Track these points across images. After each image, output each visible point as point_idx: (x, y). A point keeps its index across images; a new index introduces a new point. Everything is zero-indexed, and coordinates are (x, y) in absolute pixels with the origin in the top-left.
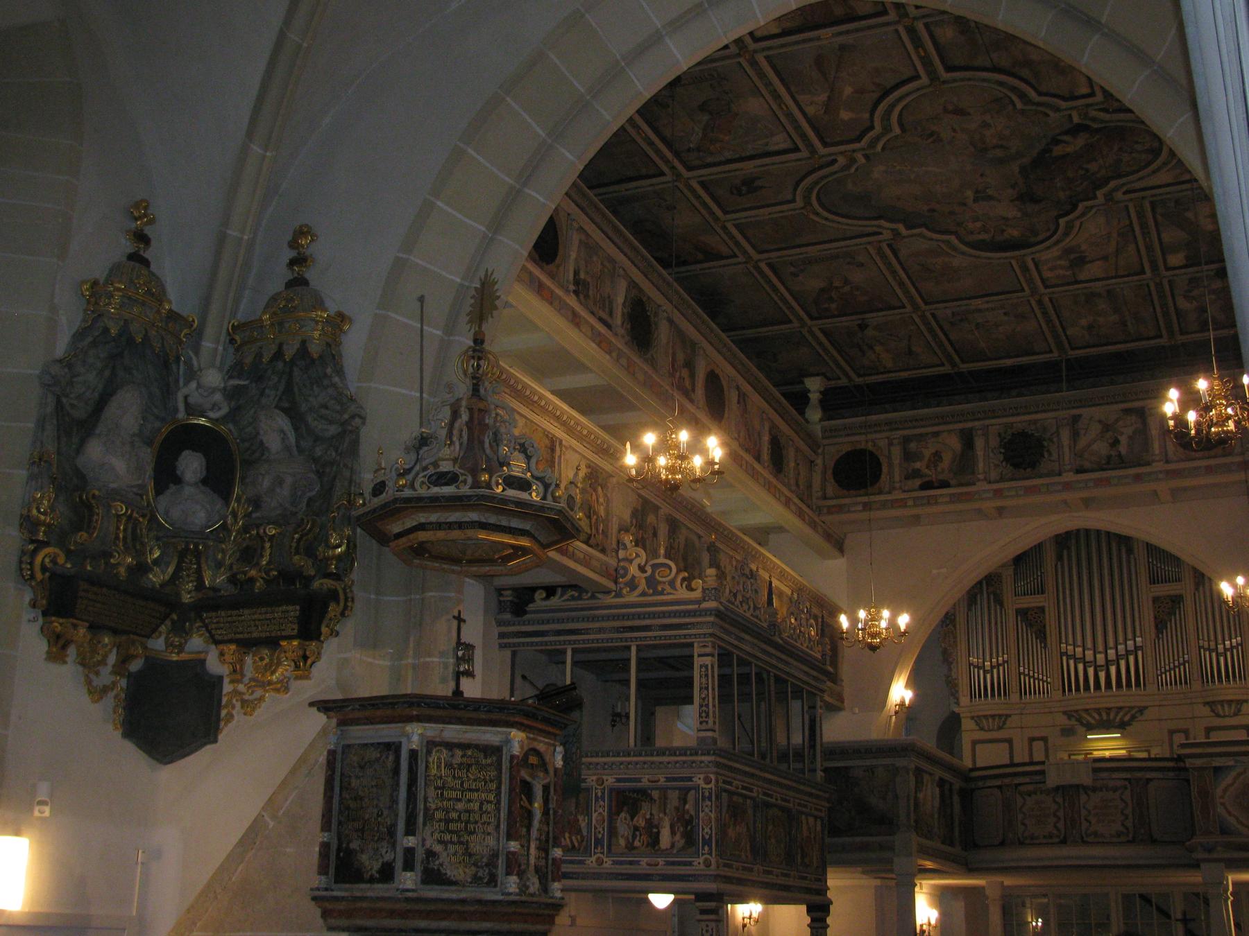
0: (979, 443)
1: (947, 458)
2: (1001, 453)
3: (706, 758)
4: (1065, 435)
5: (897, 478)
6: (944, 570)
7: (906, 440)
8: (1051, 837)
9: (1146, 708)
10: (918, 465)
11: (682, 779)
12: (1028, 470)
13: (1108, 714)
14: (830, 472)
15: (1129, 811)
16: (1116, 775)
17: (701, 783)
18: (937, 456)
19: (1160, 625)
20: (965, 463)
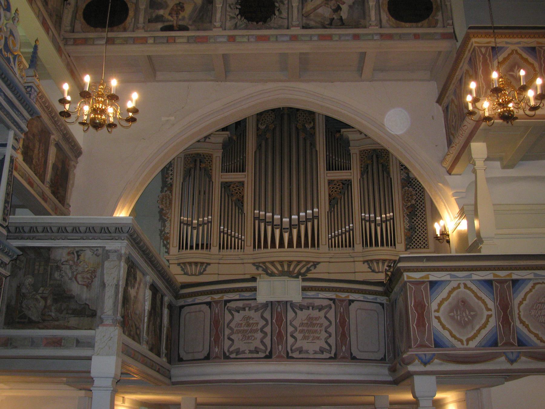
1: (189, 9)
2: (237, 8)
5: (141, 20)
6: (172, 118)
8: (257, 352)
9: (319, 263)
10: (161, 12)
12: (261, 23)
13: (289, 266)
15: (332, 329)
16: (322, 295)
19: (333, 201)
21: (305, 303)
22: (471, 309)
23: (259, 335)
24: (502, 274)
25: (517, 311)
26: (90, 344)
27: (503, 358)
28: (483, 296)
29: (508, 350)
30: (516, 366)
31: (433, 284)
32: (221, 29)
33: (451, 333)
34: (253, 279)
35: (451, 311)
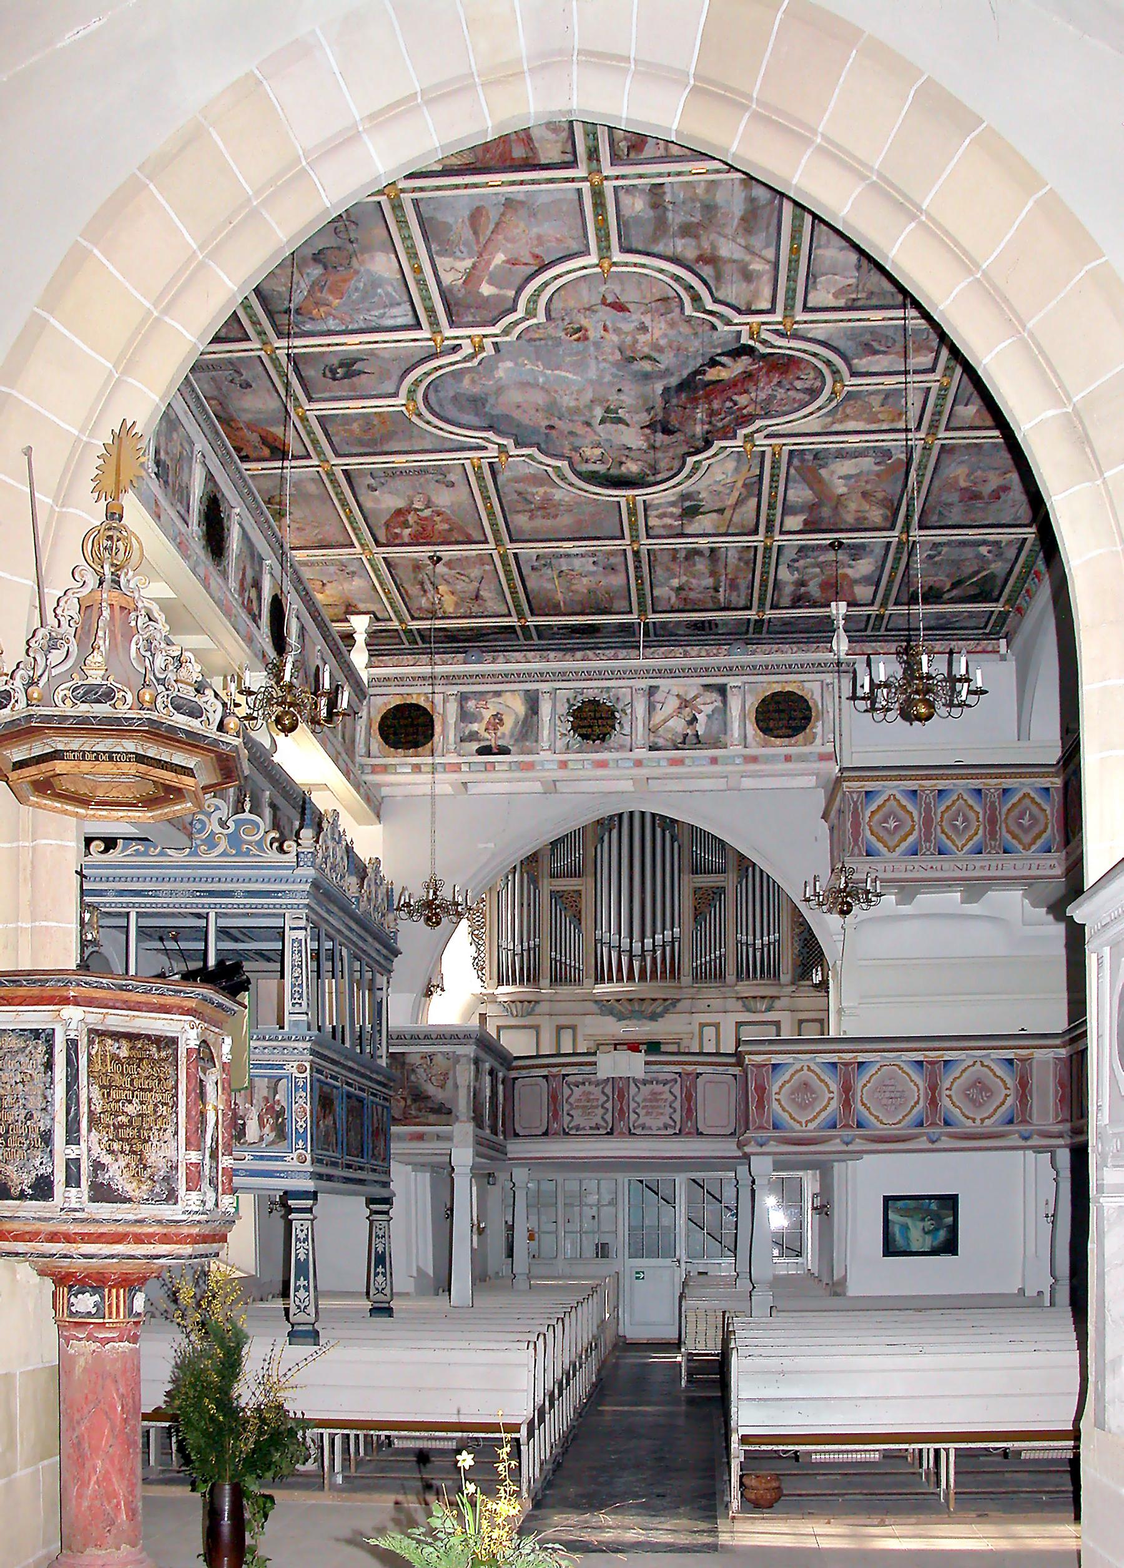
0: (545, 708)
3: (300, 1045)
4: (640, 708)
7: (463, 698)
10: (475, 727)
11: (272, 1067)
12: (598, 742)
14: (376, 726)
15: (677, 1105)
17: (294, 1070)
18: (498, 718)
20: (528, 727)
21: (648, 1077)
22: (813, 1092)
23: (600, 1111)
24: (847, 1057)
25: (859, 1094)
26: (449, 1138)
27: (838, 1140)
28: (827, 1080)
29: (844, 1133)
30: (850, 1148)
31: (775, 1066)
32: (549, 752)
33: (791, 1116)
34: (595, 1054)
35: (793, 1093)
